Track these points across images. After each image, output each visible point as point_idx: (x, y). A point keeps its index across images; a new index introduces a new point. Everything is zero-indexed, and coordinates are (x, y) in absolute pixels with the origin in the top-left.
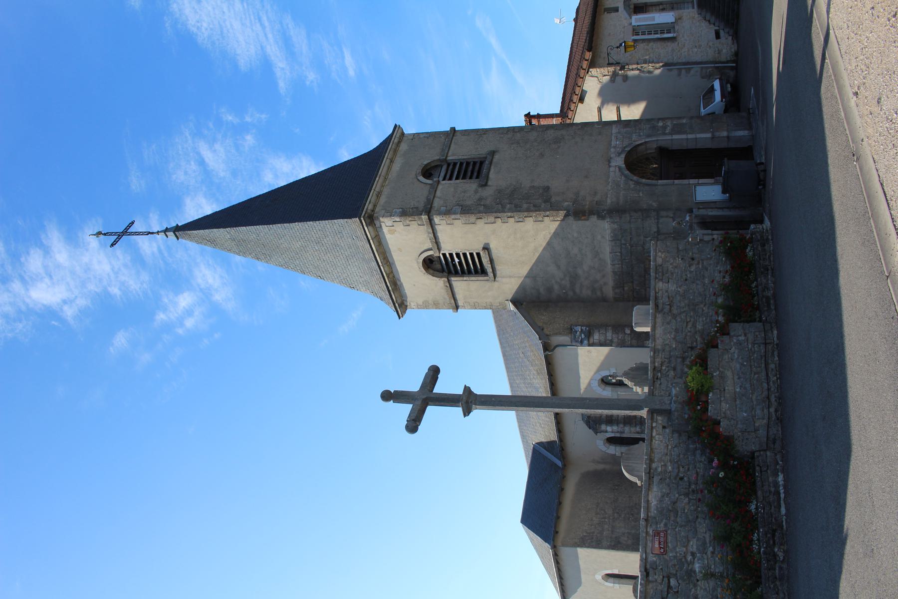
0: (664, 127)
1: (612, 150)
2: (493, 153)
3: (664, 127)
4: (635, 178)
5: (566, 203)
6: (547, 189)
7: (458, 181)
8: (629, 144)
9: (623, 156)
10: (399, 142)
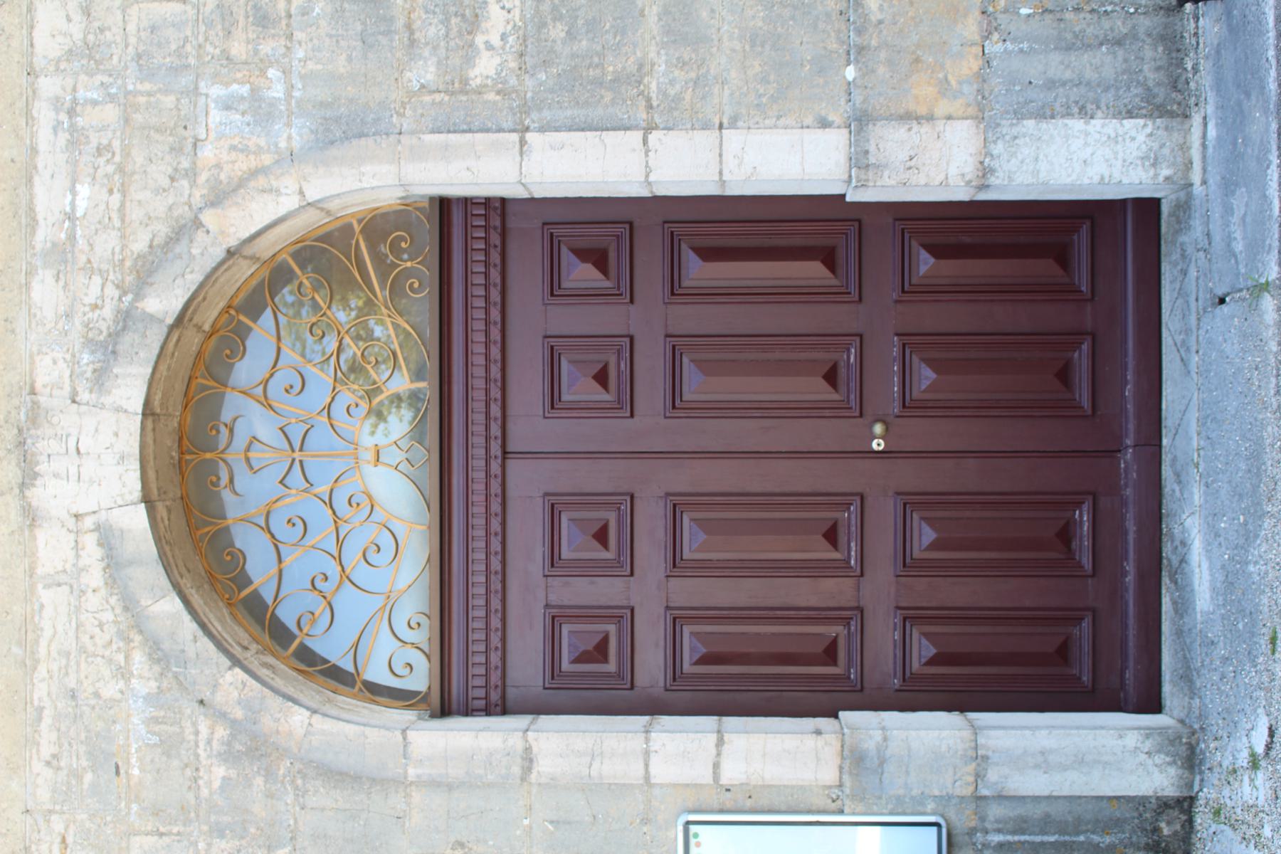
1: (45, 292)
4: (232, 685)
9: (130, 390)
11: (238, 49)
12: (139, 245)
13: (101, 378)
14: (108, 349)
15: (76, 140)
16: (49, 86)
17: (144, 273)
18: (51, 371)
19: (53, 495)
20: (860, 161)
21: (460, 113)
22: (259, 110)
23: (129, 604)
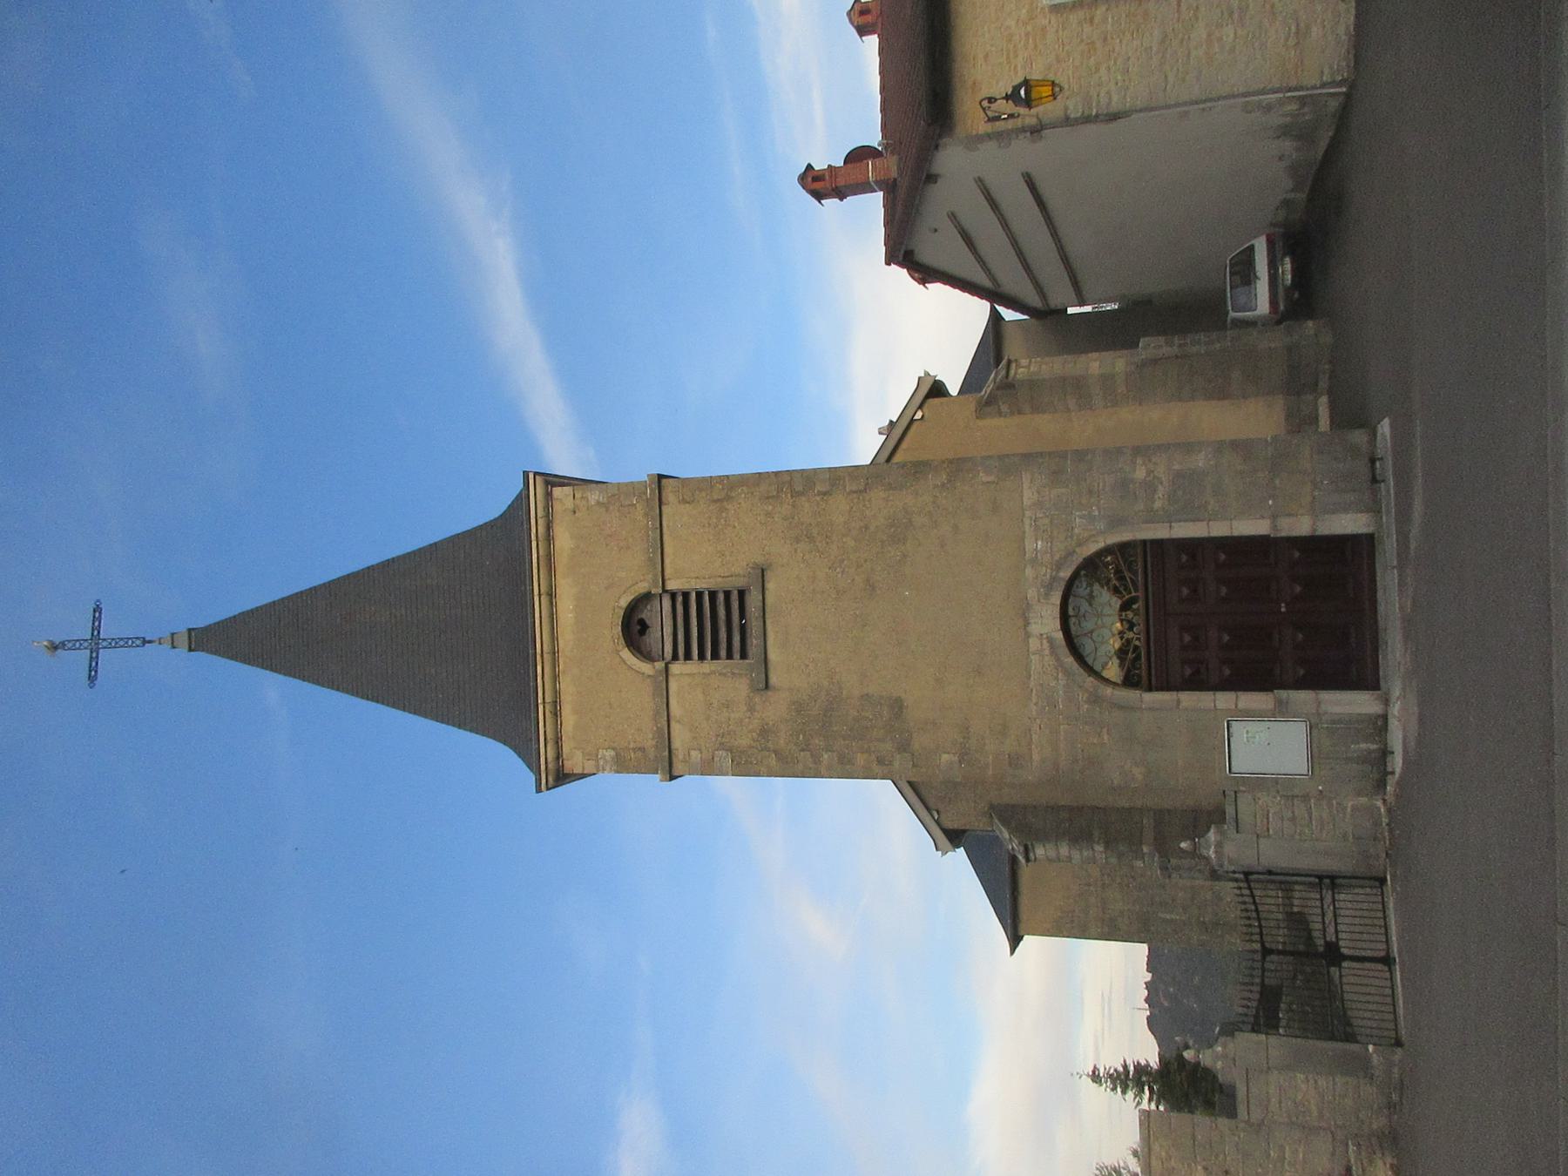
0: (1150, 487)
1: (1029, 572)
2: (762, 573)
3: (1150, 487)
5: (945, 757)
6: (898, 706)
7: (708, 666)
8: (1071, 553)
10: (549, 527)
11: (1084, 501)
12: (1057, 557)
13: (1047, 595)
14: (1049, 587)
15: (1037, 528)
16: (1028, 513)
17: (1059, 566)
18: (1032, 593)
19: (1035, 628)
20: (1274, 527)
21: (1152, 518)
22: (1091, 519)
23: (1058, 660)
